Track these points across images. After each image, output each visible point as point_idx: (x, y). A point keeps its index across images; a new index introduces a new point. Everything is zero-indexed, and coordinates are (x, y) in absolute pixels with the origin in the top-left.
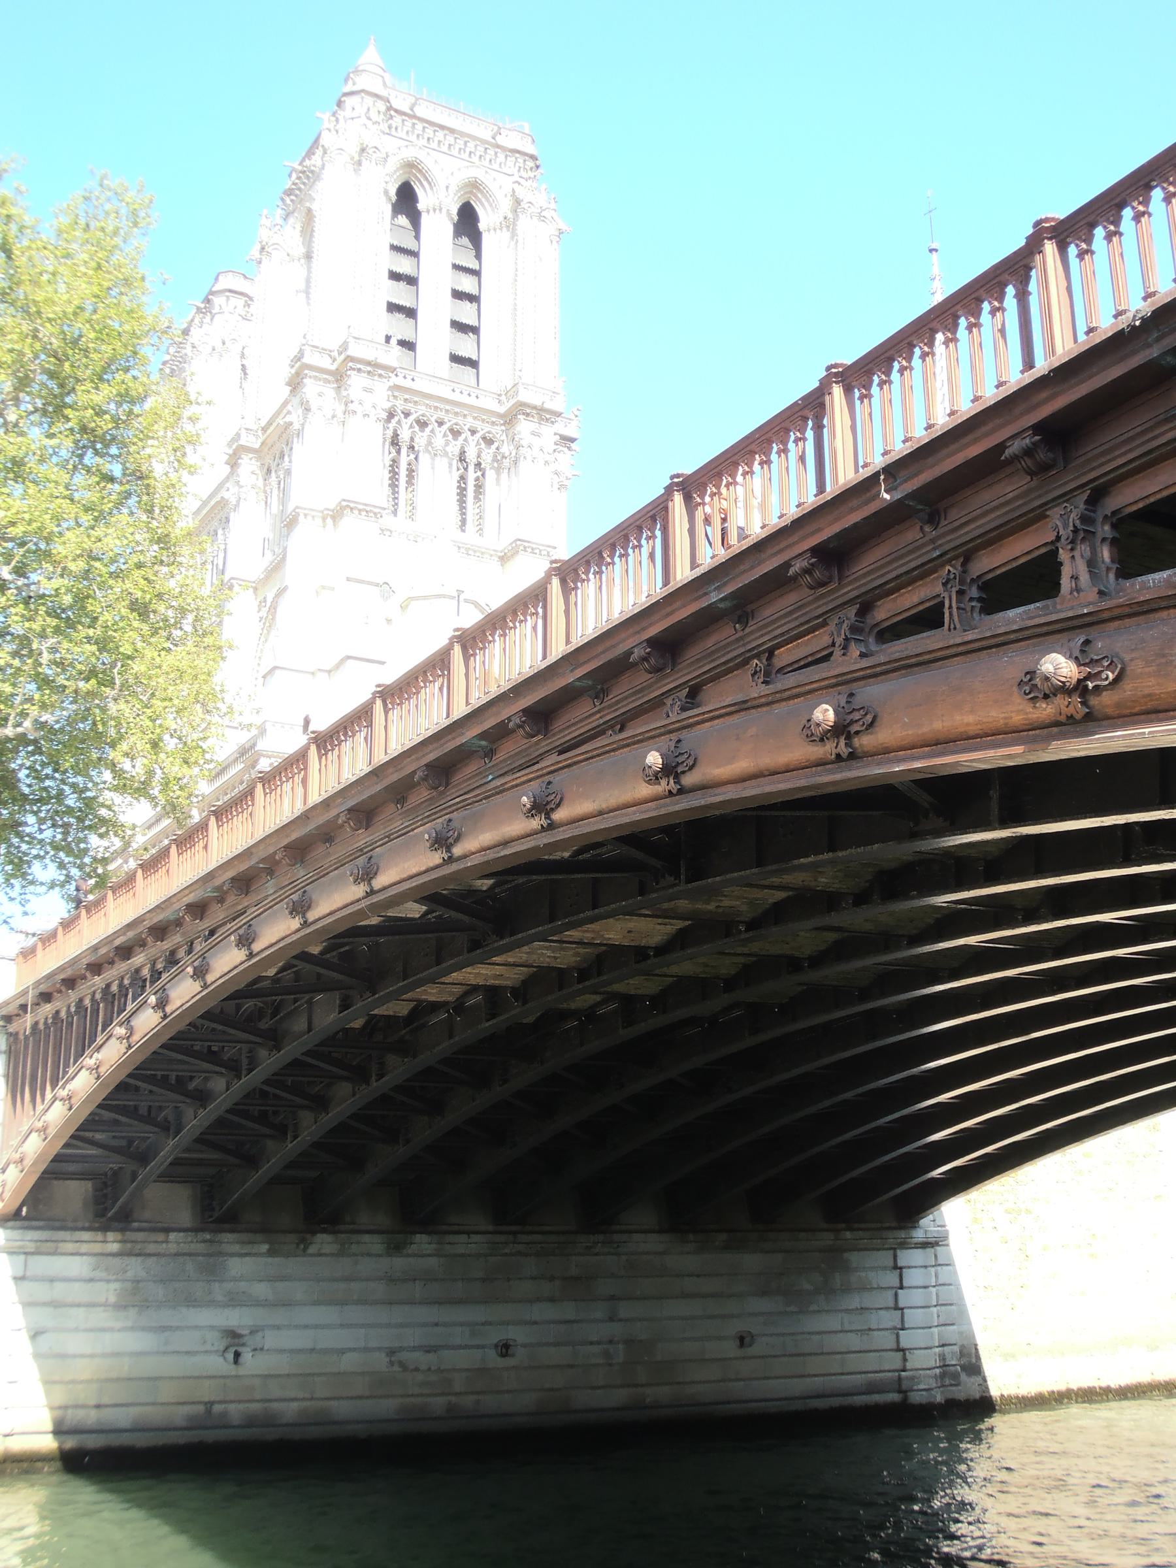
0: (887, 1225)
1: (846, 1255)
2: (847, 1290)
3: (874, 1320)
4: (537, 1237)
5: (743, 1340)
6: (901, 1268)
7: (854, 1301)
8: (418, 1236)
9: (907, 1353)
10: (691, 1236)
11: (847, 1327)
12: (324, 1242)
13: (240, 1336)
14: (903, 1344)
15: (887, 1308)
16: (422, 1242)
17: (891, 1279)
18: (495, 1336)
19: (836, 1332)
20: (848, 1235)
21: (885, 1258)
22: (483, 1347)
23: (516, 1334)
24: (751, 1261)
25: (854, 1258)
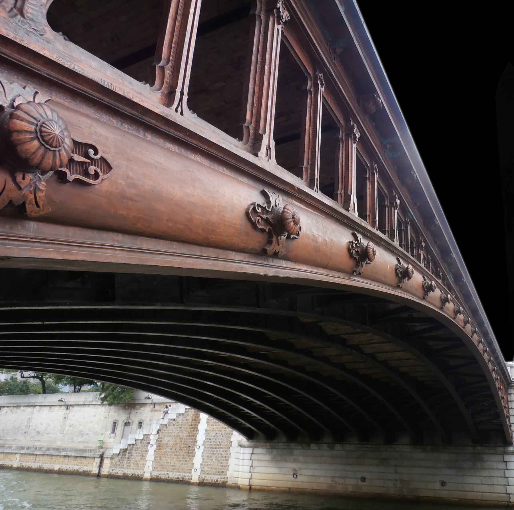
0: (499, 445)
1: (482, 456)
2: (484, 469)
3: (495, 481)
4: (370, 446)
5: (443, 484)
6: (507, 462)
7: (486, 473)
8: (336, 445)
9: (511, 496)
10: (418, 447)
11: (484, 483)
12: (313, 446)
13: (297, 471)
14: (508, 492)
15: (502, 477)
16: (338, 447)
17: (502, 466)
18: (360, 475)
19: (480, 484)
20: (479, 448)
21: (498, 458)
22: (357, 478)
23: (366, 475)
24: (444, 456)
25: (486, 457)
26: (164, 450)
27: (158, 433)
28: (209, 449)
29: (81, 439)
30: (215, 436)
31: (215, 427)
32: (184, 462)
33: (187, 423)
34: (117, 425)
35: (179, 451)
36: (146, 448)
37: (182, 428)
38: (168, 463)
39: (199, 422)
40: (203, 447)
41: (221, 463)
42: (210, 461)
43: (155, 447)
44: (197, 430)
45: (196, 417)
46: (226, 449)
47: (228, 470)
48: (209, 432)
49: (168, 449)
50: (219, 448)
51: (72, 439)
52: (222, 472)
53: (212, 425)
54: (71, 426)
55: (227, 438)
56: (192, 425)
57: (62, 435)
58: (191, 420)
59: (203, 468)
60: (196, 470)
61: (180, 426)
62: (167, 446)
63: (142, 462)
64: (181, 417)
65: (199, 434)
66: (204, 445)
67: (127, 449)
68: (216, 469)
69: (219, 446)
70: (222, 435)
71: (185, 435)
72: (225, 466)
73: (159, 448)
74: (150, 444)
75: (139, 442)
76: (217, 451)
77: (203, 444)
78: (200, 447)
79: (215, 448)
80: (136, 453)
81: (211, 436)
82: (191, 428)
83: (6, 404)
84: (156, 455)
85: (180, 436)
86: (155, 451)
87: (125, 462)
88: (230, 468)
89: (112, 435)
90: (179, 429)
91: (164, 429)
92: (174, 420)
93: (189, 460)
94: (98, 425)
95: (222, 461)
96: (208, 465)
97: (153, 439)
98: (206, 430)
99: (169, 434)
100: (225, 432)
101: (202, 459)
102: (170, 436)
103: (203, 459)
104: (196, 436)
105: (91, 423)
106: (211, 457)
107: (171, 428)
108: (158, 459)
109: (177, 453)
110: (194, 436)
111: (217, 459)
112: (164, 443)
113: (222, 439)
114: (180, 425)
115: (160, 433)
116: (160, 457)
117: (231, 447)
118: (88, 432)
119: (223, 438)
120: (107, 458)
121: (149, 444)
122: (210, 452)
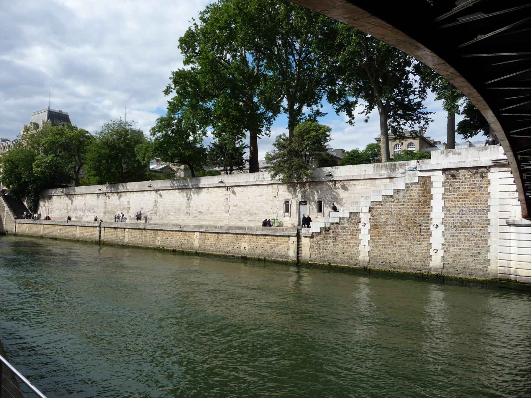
26: (383, 229)
27: (370, 211)
28: (453, 228)
29: (250, 218)
30: (459, 214)
31: (457, 203)
32: (416, 242)
33: (412, 199)
34: (290, 204)
35: (406, 230)
36: (357, 227)
37: (406, 206)
38: (392, 242)
39: (431, 199)
40: (443, 226)
41: (475, 243)
42: (456, 241)
43: (368, 226)
44: (430, 207)
45: (424, 193)
46: (481, 228)
47: (489, 251)
48: (448, 209)
49: (388, 228)
50: (468, 227)
51: (240, 218)
52: (479, 253)
53: (452, 201)
54: (235, 206)
55: (480, 215)
56: (419, 202)
57: (228, 215)
58: (417, 196)
59: (447, 248)
60: (437, 250)
61: (403, 203)
62: (388, 225)
63: (353, 241)
64: (401, 193)
65: (433, 211)
66: (443, 223)
67: (329, 228)
68: (468, 249)
69: (468, 225)
70: (471, 212)
71: (411, 213)
72: (483, 247)
73: (374, 226)
74: (362, 222)
75: (345, 220)
76: (465, 230)
77: (442, 223)
78: (437, 226)
79: (462, 227)
80: (344, 232)
81: (454, 214)
82: (418, 205)
83: (161, 187)
84: (372, 234)
85: (403, 214)
86: (370, 230)
87: (330, 241)
88: (492, 249)
89: (287, 214)
90: (400, 207)
91: (378, 206)
92: (391, 196)
93: (422, 239)
94: (267, 204)
95: (476, 241)
96: (453, 246)
97: (365, 217)
98: (444, 207)
99: (386, 212)
100: (475, 208)
101: (443, 238)
102: (389, 214)
103: (445, 239)
104: (429, 214)
105: (258, 202)
106: (457, 236)
107: (388, 206)
108: (375, 239)
109: (404, 232)
110: (425, 214)
111: (468, 240)
112: (381, 221)
113: (471, 217)
114: (401, 202)
115: (373, 211)
116: (379, 236)
117: (488, 226)
118: (257, 212)
119: (473, 215)
120: (306, 237)
121: (360, 222)
122: (454, 231)
